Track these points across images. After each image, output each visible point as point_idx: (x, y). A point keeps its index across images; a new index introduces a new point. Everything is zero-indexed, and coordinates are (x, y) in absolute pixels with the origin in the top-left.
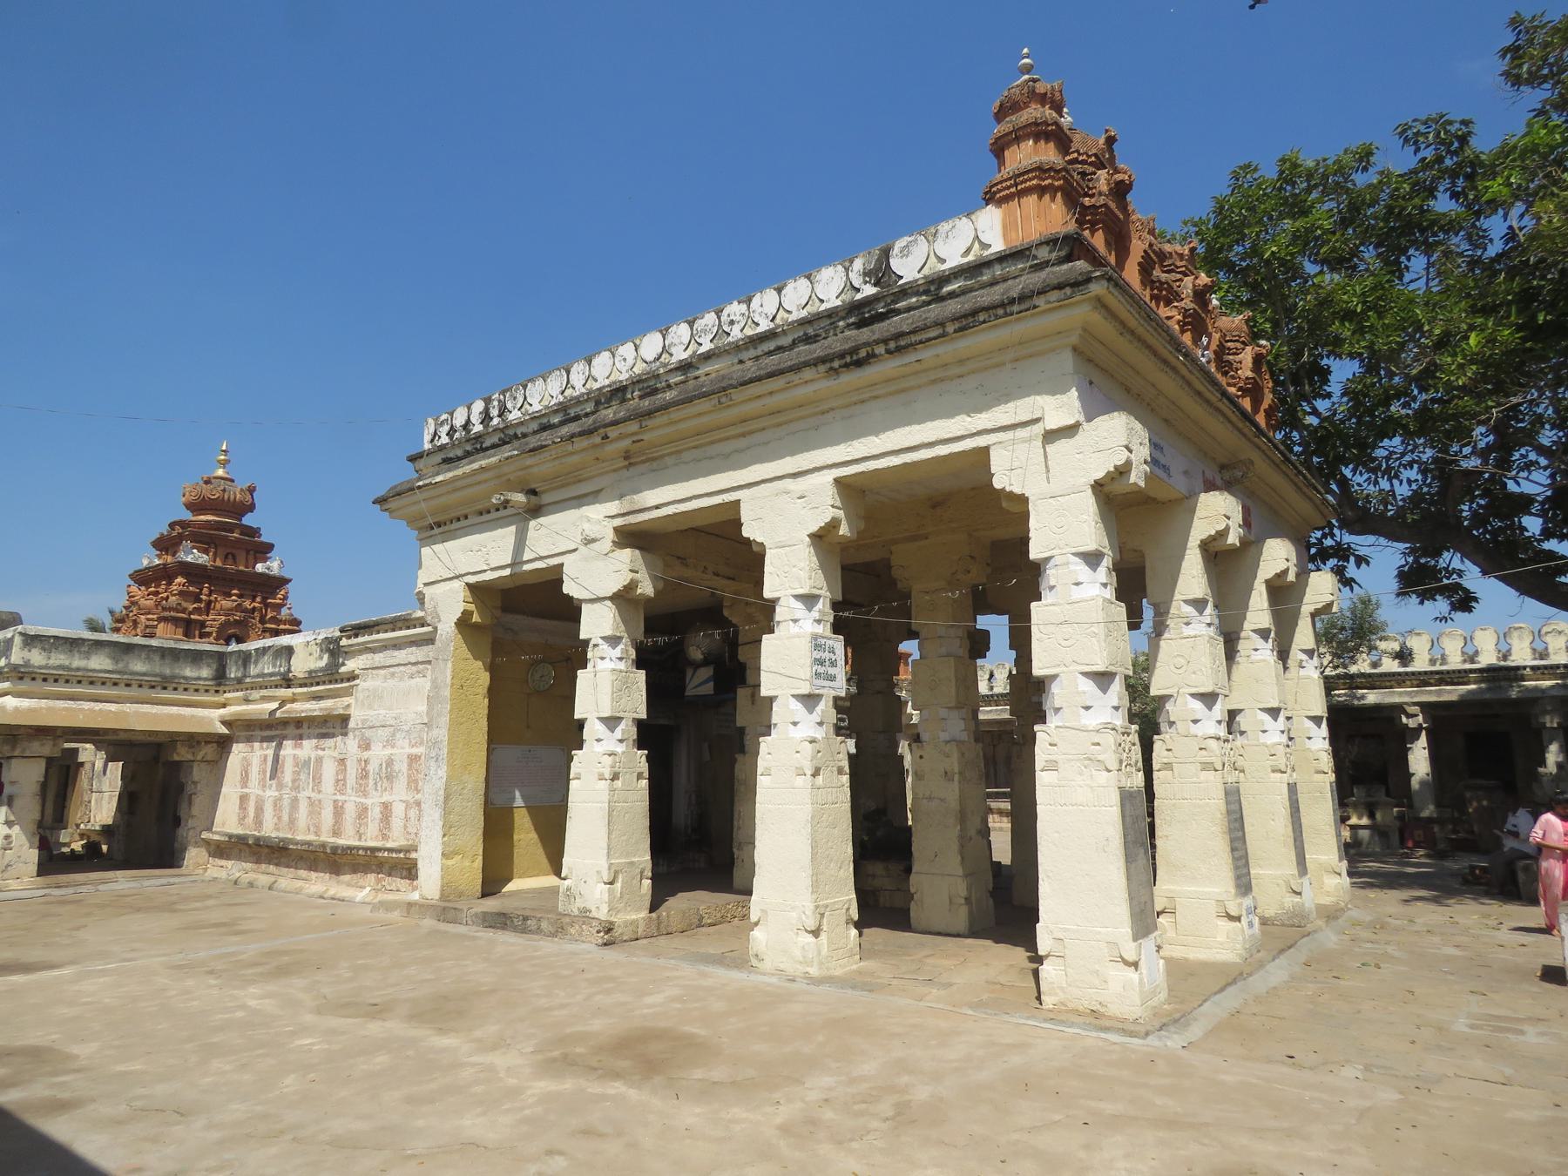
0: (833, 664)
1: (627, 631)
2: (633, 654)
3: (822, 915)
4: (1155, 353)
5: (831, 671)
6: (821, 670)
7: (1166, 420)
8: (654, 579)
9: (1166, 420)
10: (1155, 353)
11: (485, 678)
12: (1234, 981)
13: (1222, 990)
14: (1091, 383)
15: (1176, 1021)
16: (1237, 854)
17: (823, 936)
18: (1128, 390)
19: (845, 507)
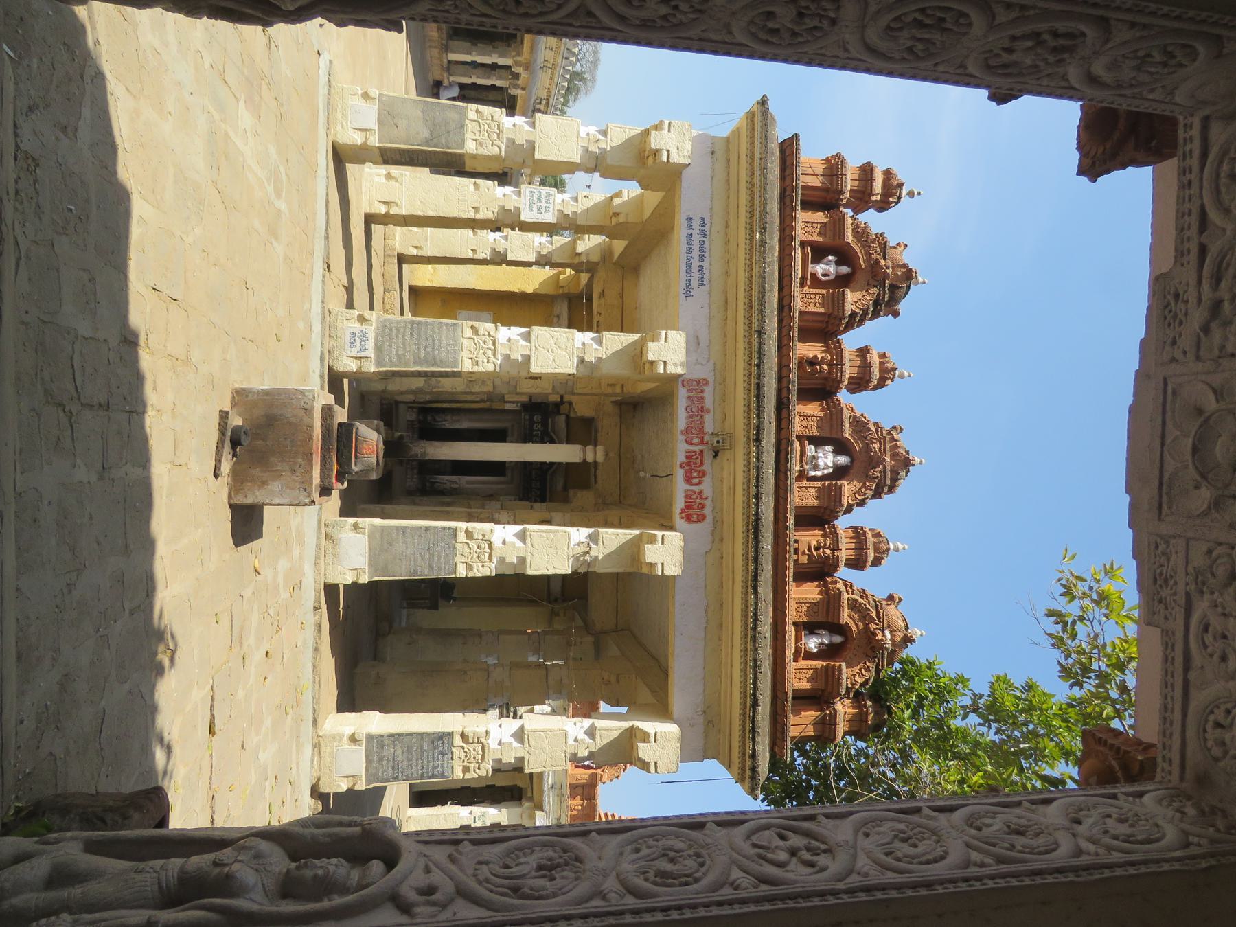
0: (539, 209)
1: (557, 249)
2: (544, 252)
3: (397, 180)
4: (752, 213)
5: (535, 208)
6: (535, 196)
7: (726, 301)
8: (588, 253)
9: (726, 301)
10: (752, 213)
11: (530, 290)
12: (327, 238)
13: (327, 202)
14: (712, 153)
15: (328, 103)
16: (408, 332)
17: (383, 180)
18: (727, 226)
19: (629, 200)
